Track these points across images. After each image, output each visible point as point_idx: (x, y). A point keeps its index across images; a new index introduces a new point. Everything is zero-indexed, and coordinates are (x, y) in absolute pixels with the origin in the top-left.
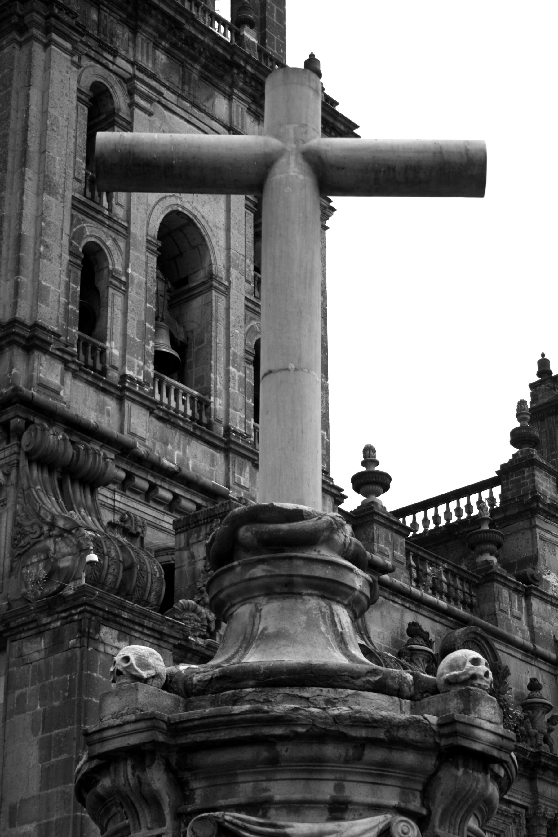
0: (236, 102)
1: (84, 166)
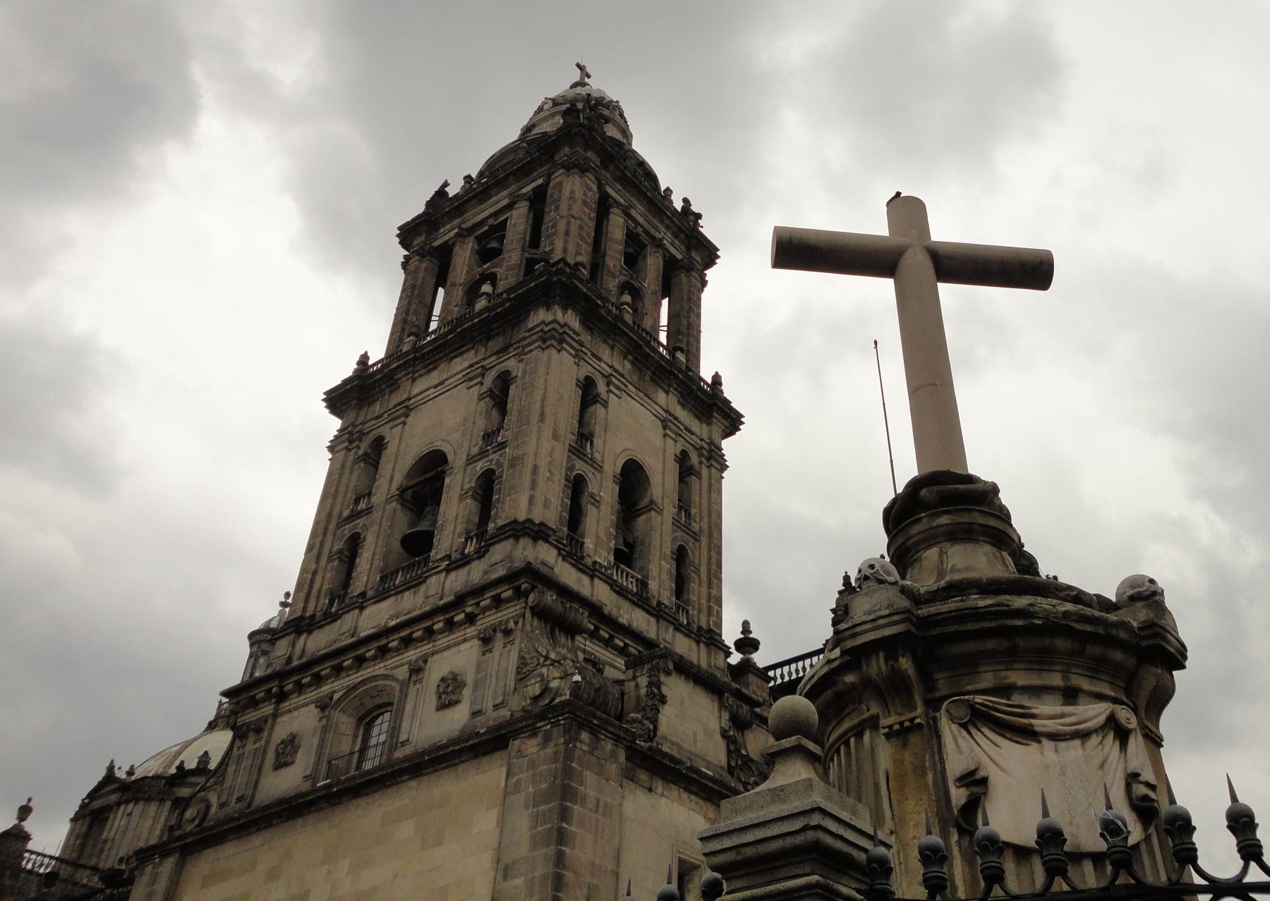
0: (671, 396)
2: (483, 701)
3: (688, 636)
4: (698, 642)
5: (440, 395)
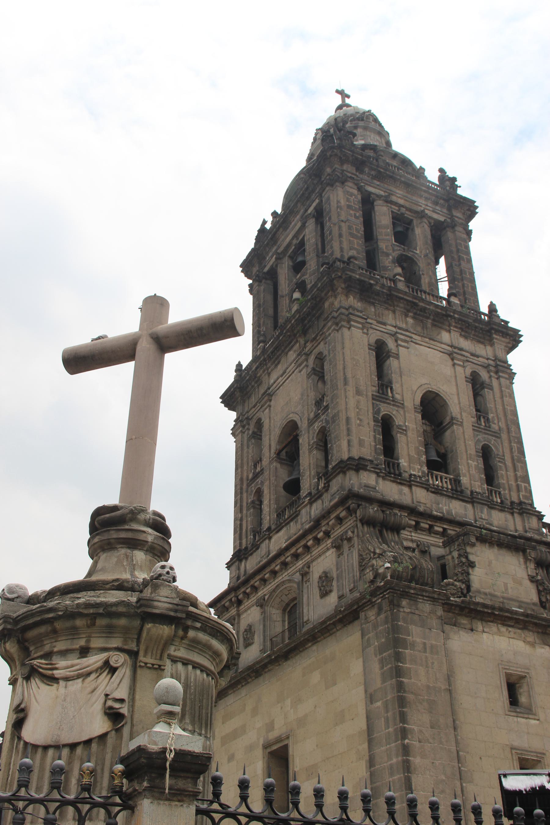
0: (453, 333)
1: (377, 379)
2: (343, 589)
3: (501, 511)
4: (512, 514)
5: (285, 381)
